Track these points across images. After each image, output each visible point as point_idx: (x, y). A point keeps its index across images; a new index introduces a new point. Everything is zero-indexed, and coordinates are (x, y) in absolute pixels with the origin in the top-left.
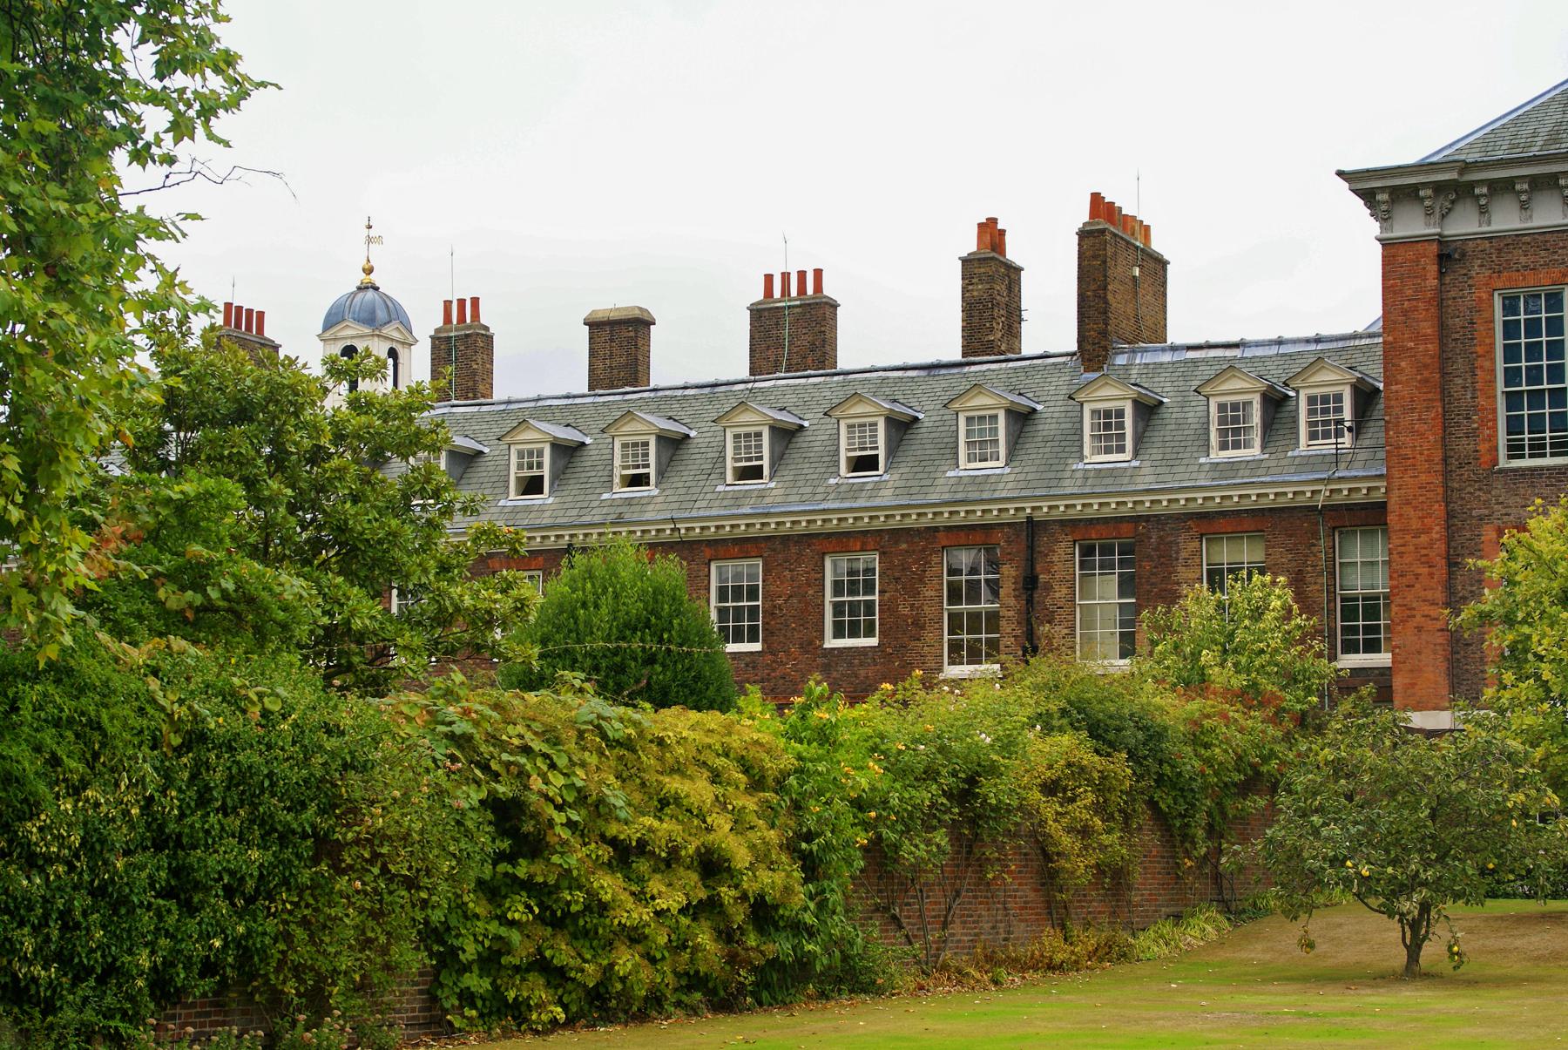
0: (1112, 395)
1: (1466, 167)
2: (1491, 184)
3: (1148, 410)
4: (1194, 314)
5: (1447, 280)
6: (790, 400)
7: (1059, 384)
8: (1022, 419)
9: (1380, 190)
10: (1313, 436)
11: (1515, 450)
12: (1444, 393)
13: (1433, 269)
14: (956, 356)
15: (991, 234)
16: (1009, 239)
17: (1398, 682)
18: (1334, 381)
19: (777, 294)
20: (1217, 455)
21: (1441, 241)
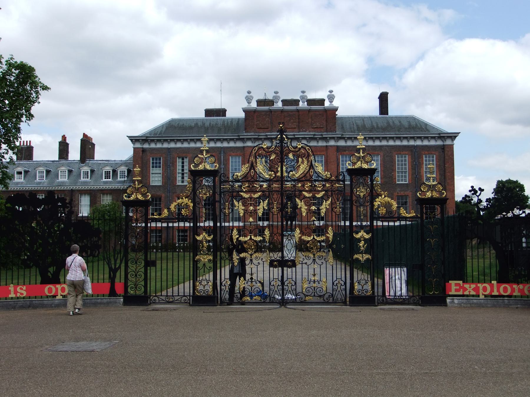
0: (86, 169)
1: (147, 137)
2: (151, 140)
3: (92, 171)
4: (99, 155)
6: (26, 166)
7: (77, 166)
8: (70, 172)
9: (134, 140)
10: (120, 178)
13: (141, 153)
14: (57, 159)
15: (64, 138)
16: (67, 138)
18: (124, 169)
19: (22, 144)
20: (104, 180)
21: (143, 148)
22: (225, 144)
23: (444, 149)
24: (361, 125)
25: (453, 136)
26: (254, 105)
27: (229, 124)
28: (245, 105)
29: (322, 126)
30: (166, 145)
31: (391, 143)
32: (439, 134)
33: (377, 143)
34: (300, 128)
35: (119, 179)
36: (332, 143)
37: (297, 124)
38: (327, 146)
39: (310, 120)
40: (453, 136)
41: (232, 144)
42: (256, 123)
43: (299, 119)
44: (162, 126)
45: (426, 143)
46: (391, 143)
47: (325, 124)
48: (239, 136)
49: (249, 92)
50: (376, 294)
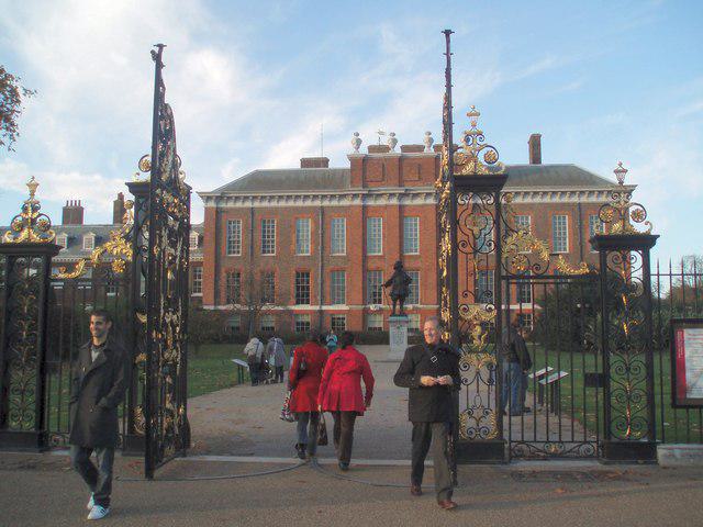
17: (204, 300)
26: (363, 150)
28: (352, 151)
50: (506, 435)
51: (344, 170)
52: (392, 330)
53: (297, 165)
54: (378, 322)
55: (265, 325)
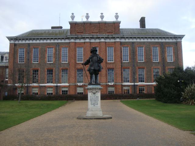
1: (17, 37)
5: (15, 47)
9: (10, 39)
11: (20, 62)
12: (14, 57)
13: (14, 46)
22: (59, 41)
23: (177, 44)
24: (132, 34)
25: (181, 37)
27: (62, 32)
28: (71, 20)
29: (112, 31)
30: (27, 42)
31: (149, 40)
32: (175, 36)
33: (142, 40)
34: (100, 32)
35: (4, 61)
36: (118, 40)
37: (99, 30)
38: (115, 42)
39: (106, 28)
40: (181, 37)
41: (63, 41)
42: (76, 30)
43: (100, 28)
44: (27, 33)
45: (167, 40)
46: (149, 40)
47: (114, 30)
48: (67, 36)
49: (73, 14)
51: (68, 30)
52: (90, 95)
53: (50, 28)
54: (80, 90)
55: (34, 92)
